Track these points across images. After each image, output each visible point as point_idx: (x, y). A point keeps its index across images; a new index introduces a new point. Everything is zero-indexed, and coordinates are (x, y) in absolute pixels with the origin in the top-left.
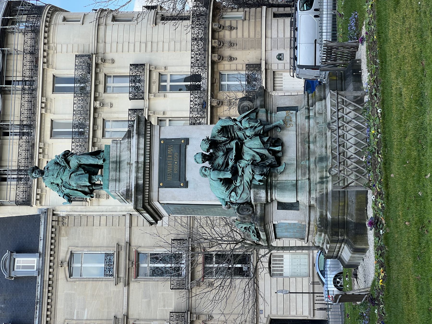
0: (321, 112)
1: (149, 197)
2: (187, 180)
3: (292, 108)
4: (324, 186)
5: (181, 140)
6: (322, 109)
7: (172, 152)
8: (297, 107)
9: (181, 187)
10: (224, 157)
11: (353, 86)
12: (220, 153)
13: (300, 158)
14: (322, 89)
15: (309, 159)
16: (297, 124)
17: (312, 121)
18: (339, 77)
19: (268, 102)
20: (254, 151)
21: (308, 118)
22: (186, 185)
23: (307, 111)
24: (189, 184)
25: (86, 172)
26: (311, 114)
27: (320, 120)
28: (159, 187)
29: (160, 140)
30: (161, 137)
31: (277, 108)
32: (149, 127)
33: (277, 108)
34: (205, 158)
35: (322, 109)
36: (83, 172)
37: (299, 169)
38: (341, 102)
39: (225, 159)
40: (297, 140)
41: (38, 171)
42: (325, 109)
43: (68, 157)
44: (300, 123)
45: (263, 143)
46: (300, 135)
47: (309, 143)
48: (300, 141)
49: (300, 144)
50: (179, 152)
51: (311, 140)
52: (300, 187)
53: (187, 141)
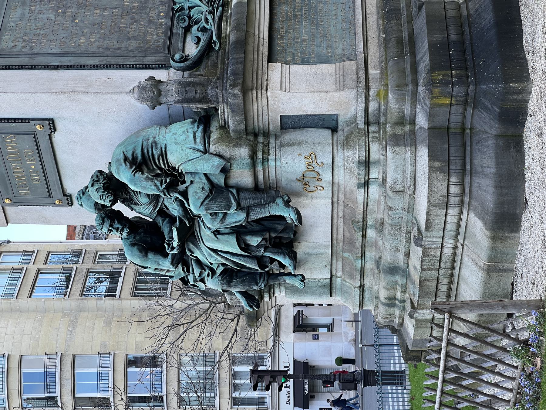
0: (401, 189)
3: (321, 116)
4: (397, 312)
6: (404, 181)
7: (15, 147)
8: (337, 116)
9: (56, 205)
10: (151, 206)
11: (498, 164)
12: (140, 199)
13: (341, 244)
14: (408, 98)
15: (363, 255)
16: (336, 181)
17: (374, 190)
18: (459, 98)
19: (255, 111)
21: (366, 184)
23: (363, 172)
26: (374, 174)
27: (399, 203)
31: (281, 116)
33: (281, 116)
35: (404, 181)
37: (337, 260)
38: (456, 195)
39: (156, 209)
40: (335, 211)
42: (412, 187)
44: (342, 182)
46: (341, 203)
47: (364, 228)
48: (341, 214)
49: (341, 221)
50: (35, 148)
51: (370, 220)
52: (338, 287)
53: (51, 124)
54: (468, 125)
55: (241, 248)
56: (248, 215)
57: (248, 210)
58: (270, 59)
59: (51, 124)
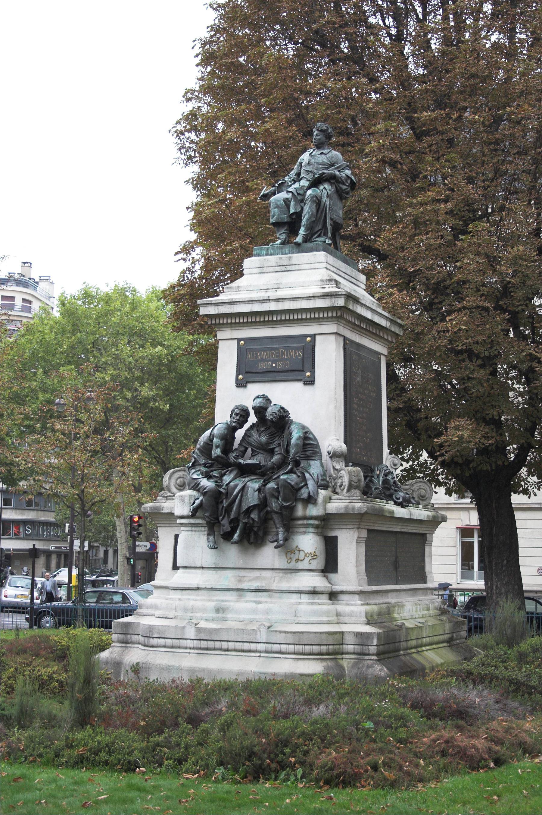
1: (219, 324)
2: (249, 386)
5: (310, 372)
9: (237, 375)
20: (236, 496)
22: (240, 384)
24: (241, 390)
25: (294, 217)
28: (239, 340)
29: (313, 336)
30: (317, 337)
32: (334, 315)
34: (260, 411)
36: (292, 211)
41: (319, 139)
43: (331, 184)
45: (249, 510)
53: (310, 382)
54: (344, 656)
55: (249, 508)
56: (276, 513)
57: (280, 513)
58: (369, 531)
59: (310, 382)
